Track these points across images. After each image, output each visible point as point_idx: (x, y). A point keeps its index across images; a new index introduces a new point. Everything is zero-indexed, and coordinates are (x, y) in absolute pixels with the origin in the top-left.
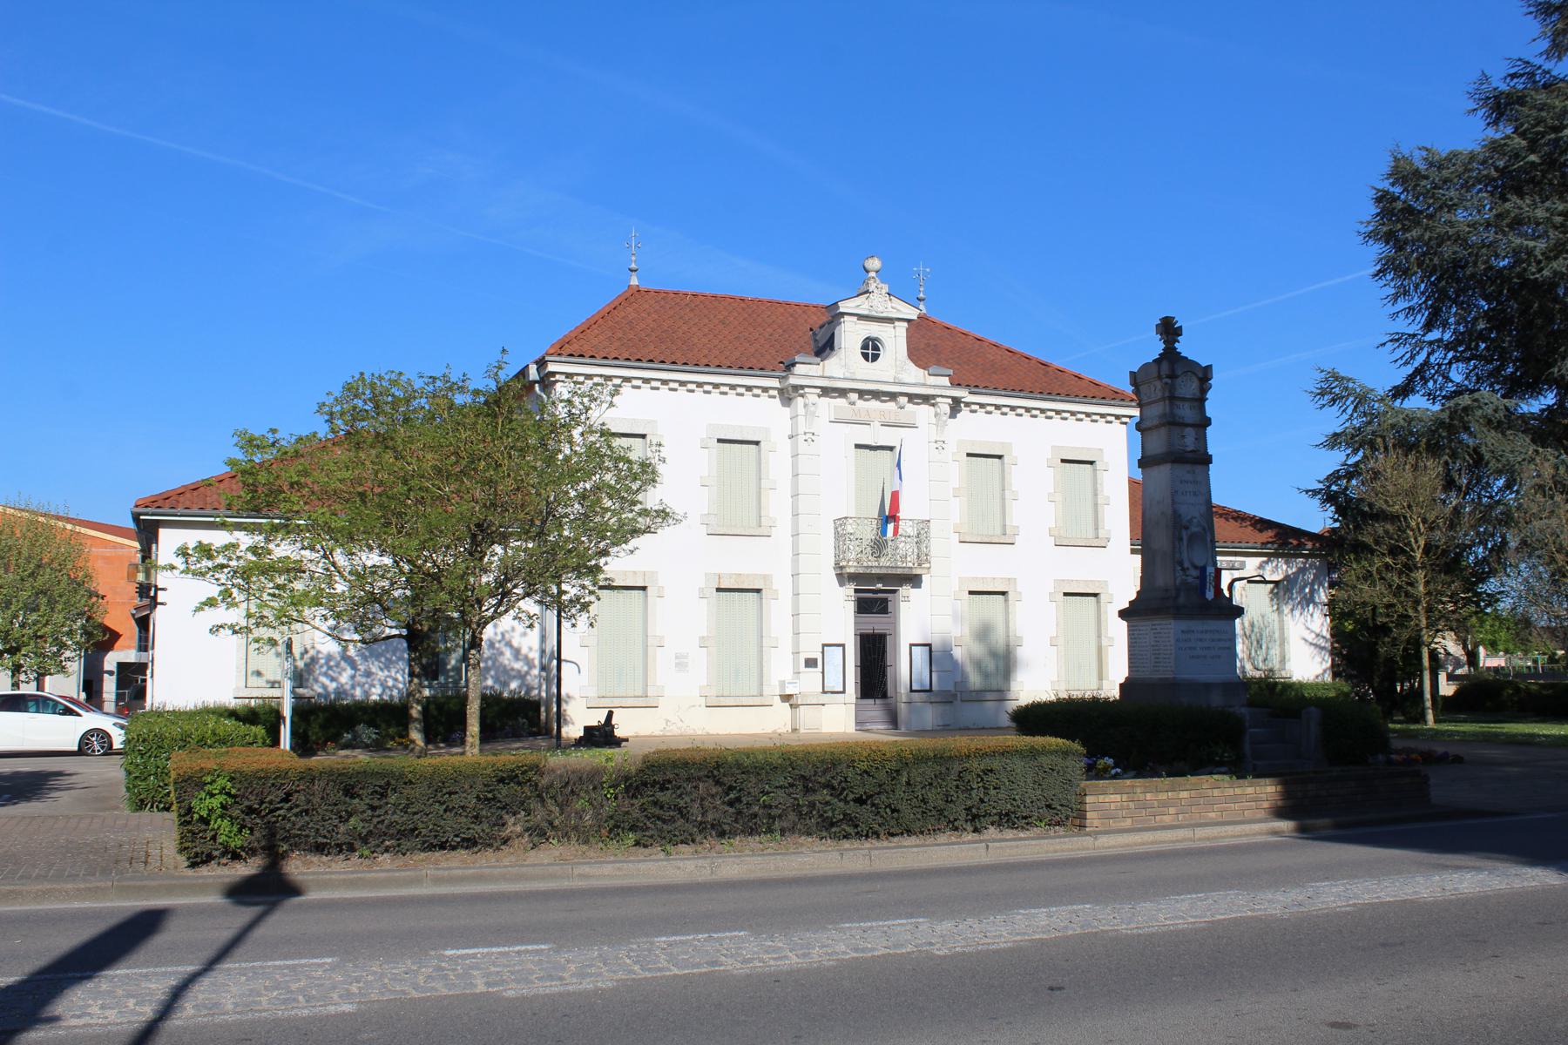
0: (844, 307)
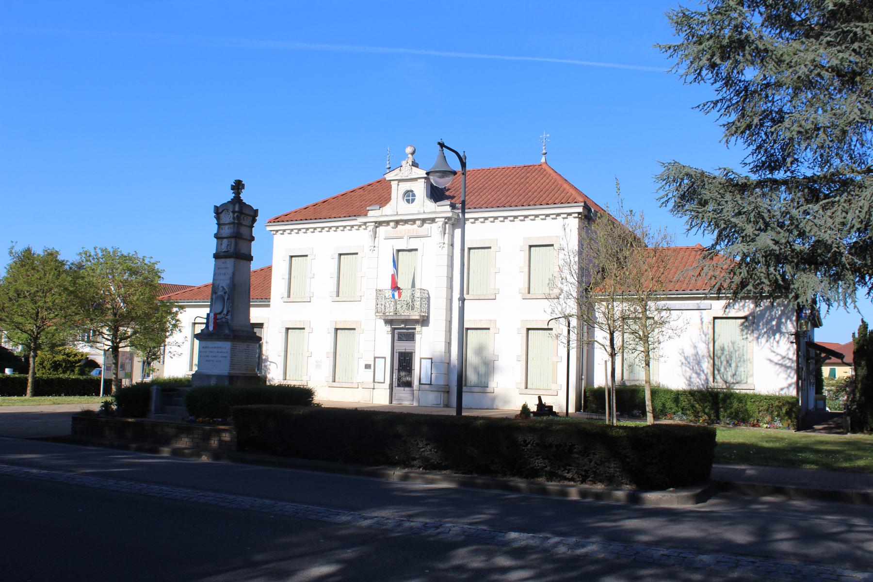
0: (389, 177)
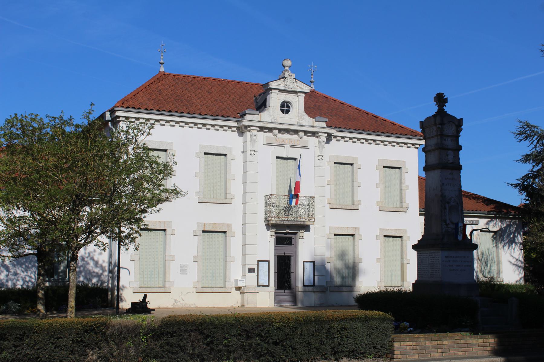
0: (272, 85)
